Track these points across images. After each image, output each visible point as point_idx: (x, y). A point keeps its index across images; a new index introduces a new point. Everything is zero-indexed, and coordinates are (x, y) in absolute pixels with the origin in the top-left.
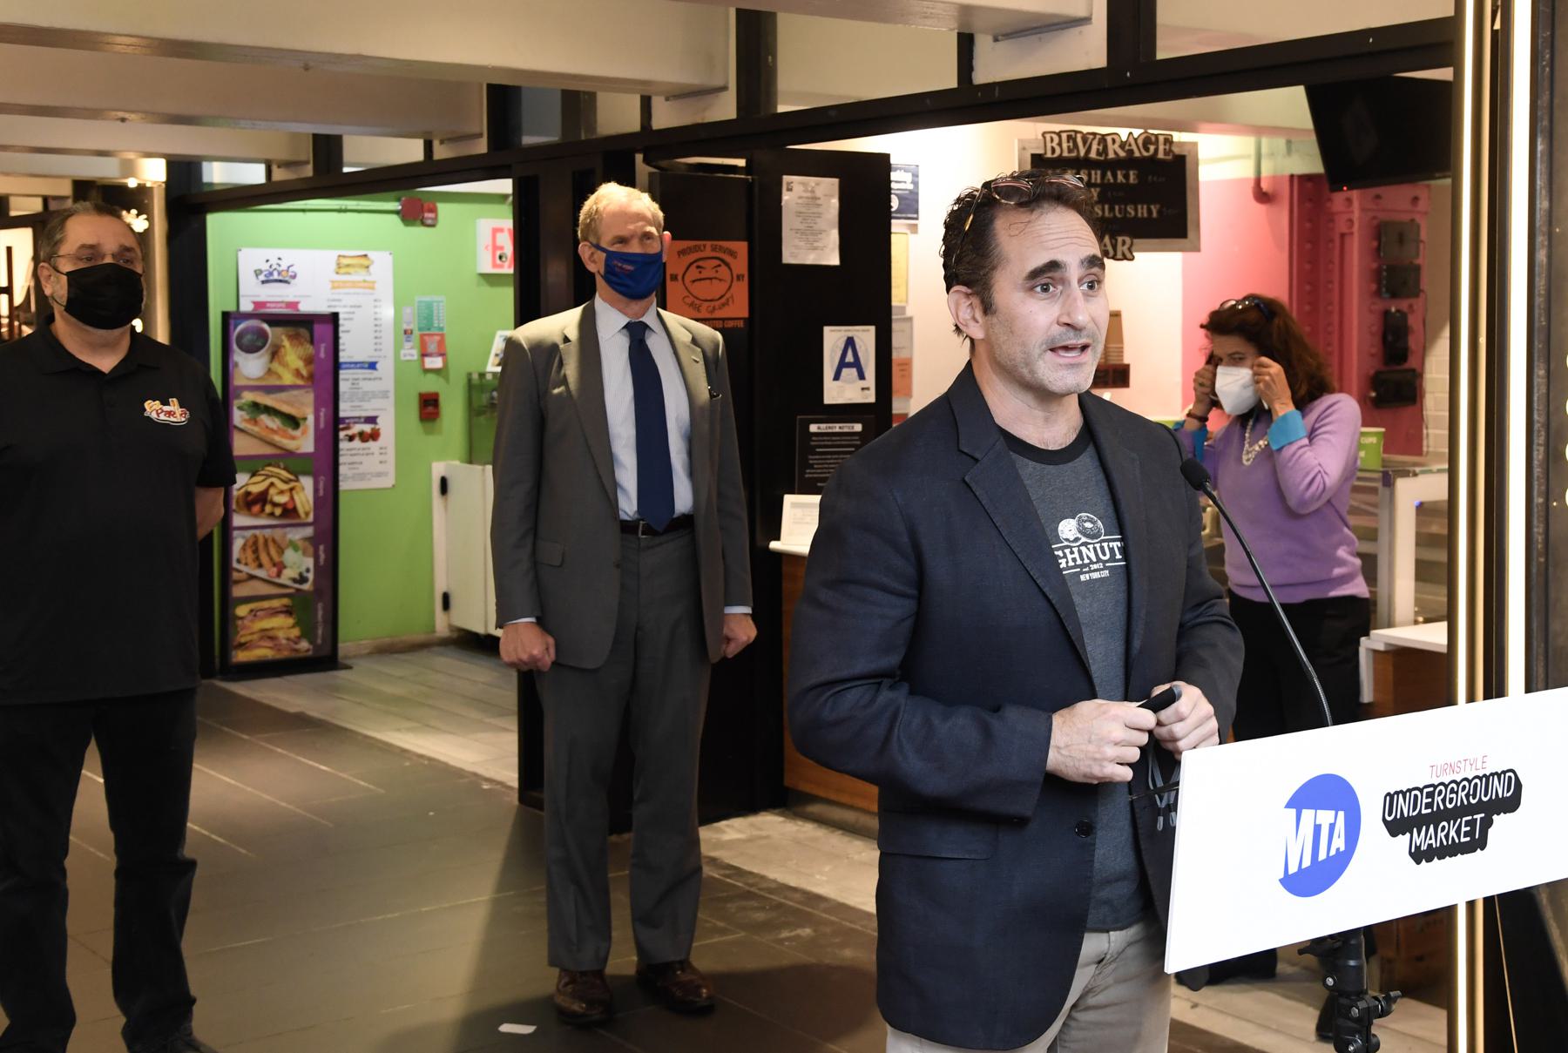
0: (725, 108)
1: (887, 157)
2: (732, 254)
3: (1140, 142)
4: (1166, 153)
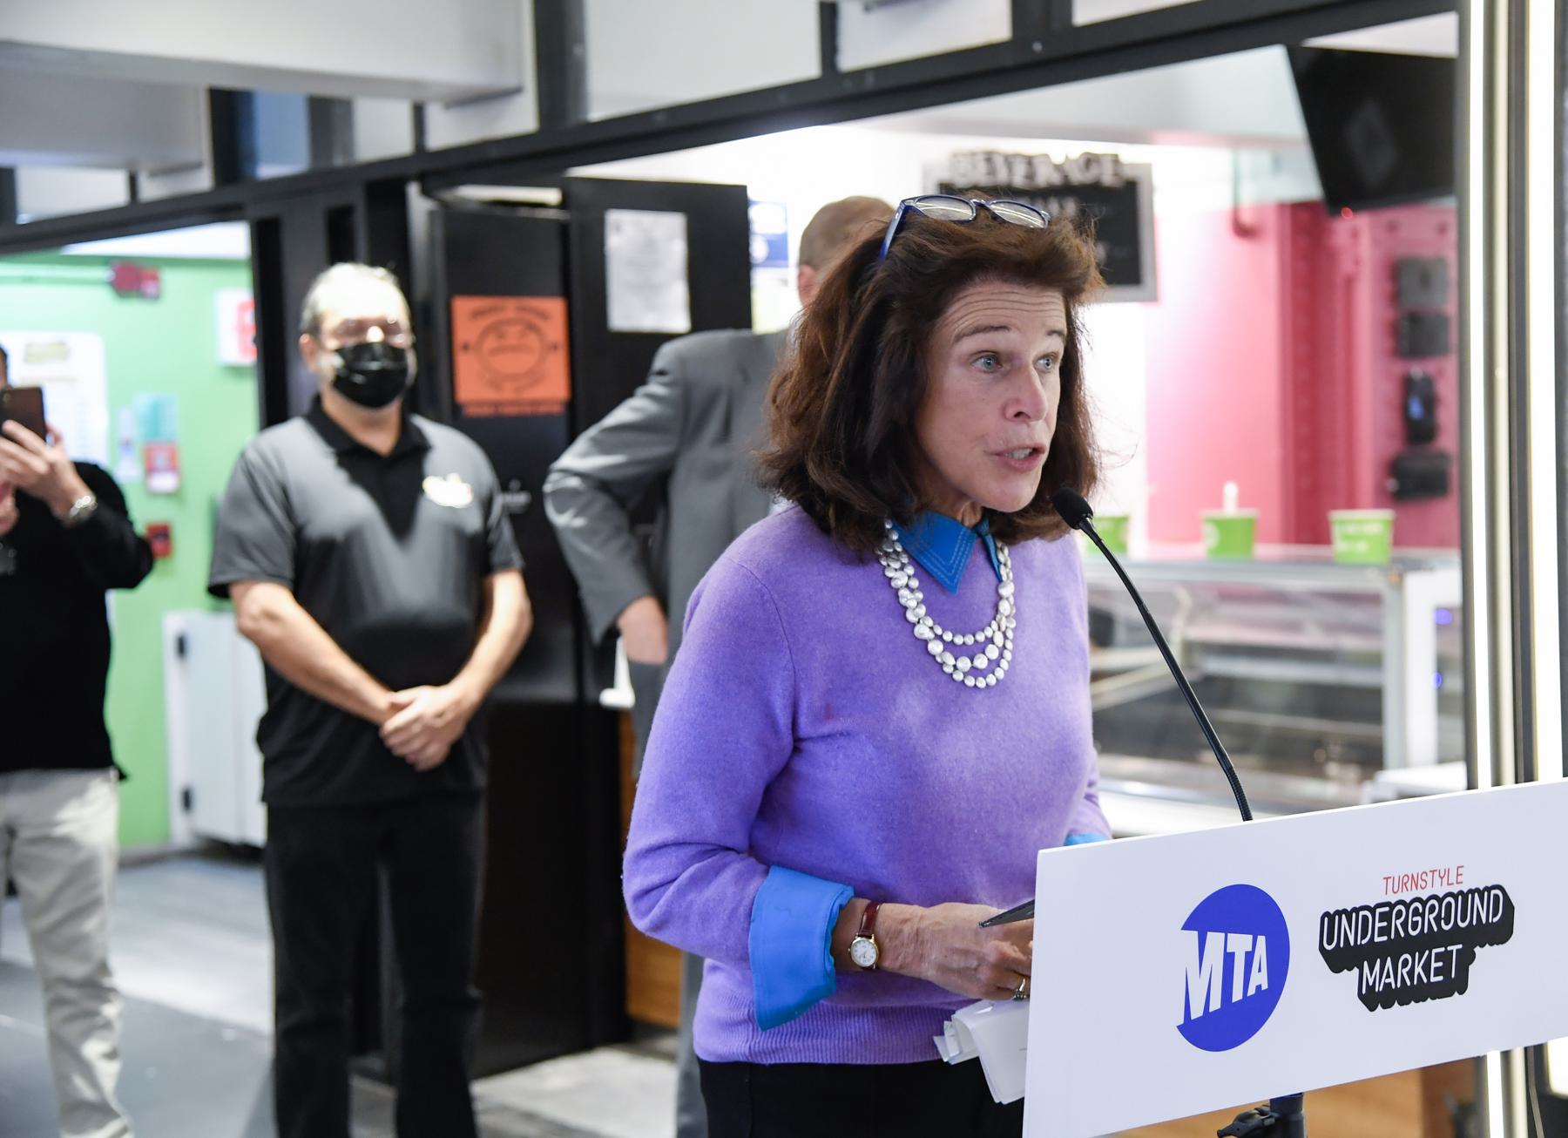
0: (521, 118)
1: (743, 189)
2: (544, 315)
3: (1082, 162)
4: (1116, 174)
